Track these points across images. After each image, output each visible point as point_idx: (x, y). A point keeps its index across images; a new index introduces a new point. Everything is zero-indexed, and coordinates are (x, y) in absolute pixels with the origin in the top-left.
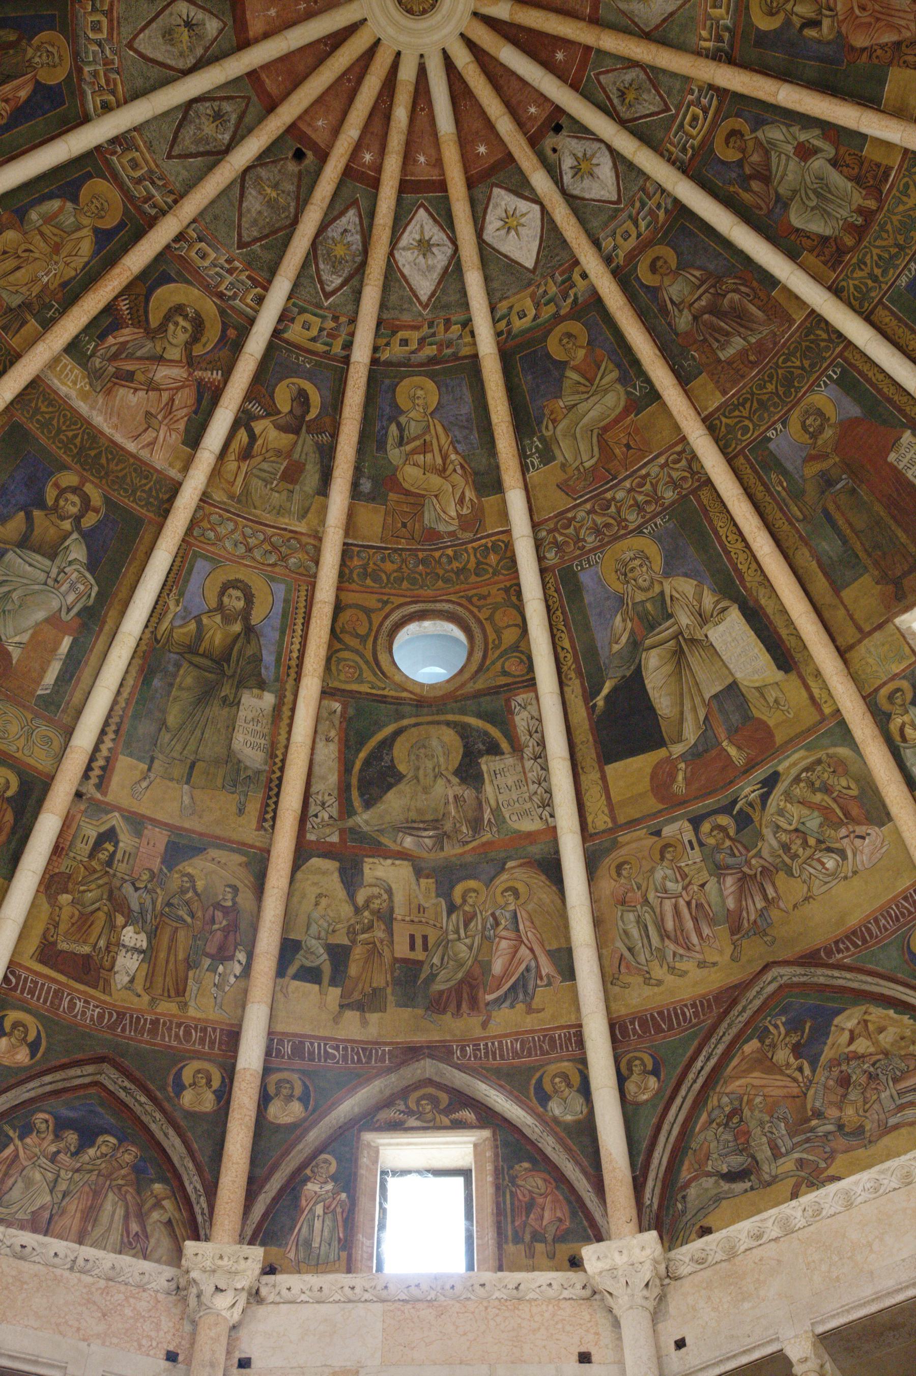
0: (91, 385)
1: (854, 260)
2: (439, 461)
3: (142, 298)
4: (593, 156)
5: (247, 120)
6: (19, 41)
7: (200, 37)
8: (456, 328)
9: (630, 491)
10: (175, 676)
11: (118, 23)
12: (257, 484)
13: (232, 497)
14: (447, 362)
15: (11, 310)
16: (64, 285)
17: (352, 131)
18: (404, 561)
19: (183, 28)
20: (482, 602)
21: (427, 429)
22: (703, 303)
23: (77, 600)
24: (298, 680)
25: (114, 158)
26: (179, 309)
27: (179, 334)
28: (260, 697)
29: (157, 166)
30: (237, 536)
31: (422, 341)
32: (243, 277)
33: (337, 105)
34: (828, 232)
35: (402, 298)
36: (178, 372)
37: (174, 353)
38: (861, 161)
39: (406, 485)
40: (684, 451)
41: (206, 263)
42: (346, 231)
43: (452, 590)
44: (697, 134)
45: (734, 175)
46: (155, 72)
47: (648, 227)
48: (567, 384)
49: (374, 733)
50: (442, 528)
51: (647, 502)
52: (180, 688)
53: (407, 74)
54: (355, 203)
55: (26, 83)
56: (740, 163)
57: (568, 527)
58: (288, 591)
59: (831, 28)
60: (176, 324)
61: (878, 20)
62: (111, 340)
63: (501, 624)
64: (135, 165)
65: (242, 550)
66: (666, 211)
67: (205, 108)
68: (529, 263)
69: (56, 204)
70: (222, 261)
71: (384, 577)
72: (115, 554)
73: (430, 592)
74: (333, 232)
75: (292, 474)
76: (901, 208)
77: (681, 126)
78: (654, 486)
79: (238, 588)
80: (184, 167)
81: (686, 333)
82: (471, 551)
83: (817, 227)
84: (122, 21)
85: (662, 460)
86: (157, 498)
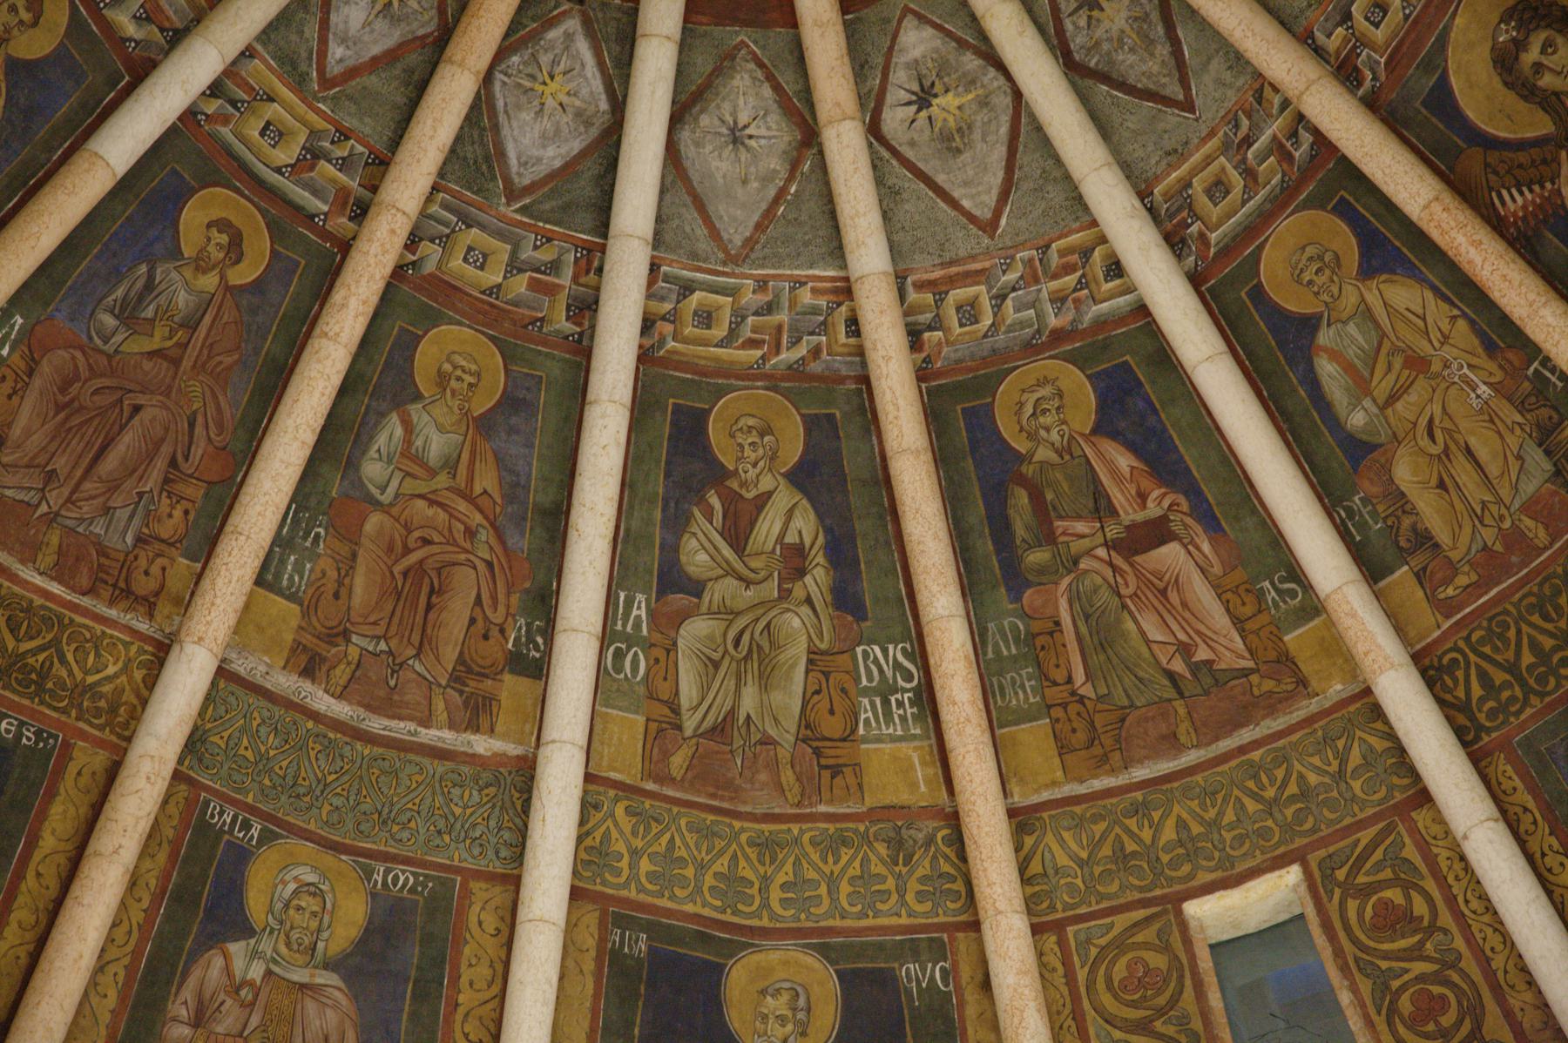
3: (1493, 157)
6: (1023, 481)
7: (943, 68)
11: (951, 263)
15: (1558, 473)
16: (1490, 348)
19: (934, 110)
25: (1213, 237)
26: (1505, 61)
29: (1212, 134)
46: (1029, 160)
55: (1101, 455)
60: (1538, 67)
64: (1219, 188)
69: (1327, 369)
80: (1205, 66)
84: (947, 256)
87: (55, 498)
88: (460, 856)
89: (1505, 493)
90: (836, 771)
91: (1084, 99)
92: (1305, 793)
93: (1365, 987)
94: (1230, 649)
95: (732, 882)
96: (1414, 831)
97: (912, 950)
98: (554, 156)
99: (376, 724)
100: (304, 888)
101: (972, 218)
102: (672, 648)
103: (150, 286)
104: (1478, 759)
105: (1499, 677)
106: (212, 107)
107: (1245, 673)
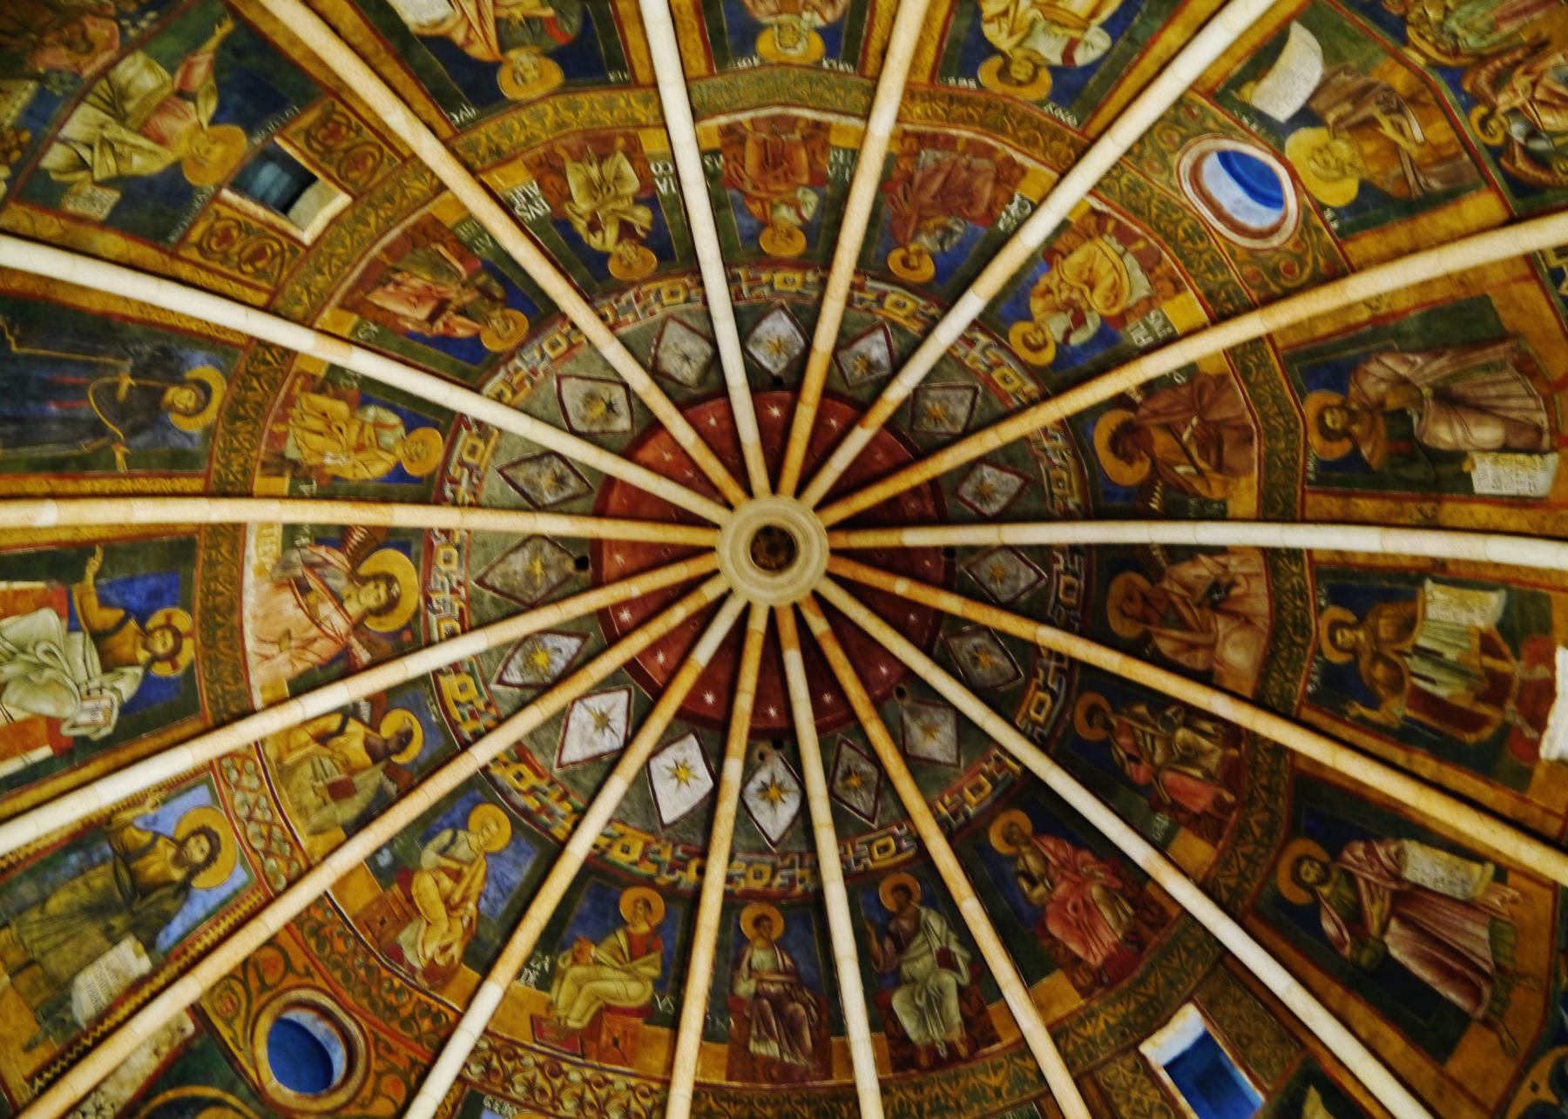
0: (274, 567)
1: (916, 1080)
2: (457, 897)
4: (786, 792)
5: (578, 505)
7: (607, 421)
8: (564, 808)
9: (586, 1081)
10: (93, 866)
12: (307, 769)
13: (279, 761)
14: (536, 825)
15: (282, 456)
16: (335, 478)
17: (635, 588)
18: (355, 953)
20: (383, 1053)
21: (471, 863)
22: (772, 989)
23: (86, 725)
24: (185, 971)
25: (465, 432)
26: (390, 579)
27: (372, 596)
28: (138, 955)
30: (251, 797)
31: (533, 790)
32: (456, 605)
33: (643, 559)
34: (914, 1036)
35: (549, 740)
36: (339, 623)
37: (353, 608)
38: (982, 1011)
39: (414, 891)
40: (657, 1092)
41: (443, 567)
42: (560, 651)
43: (370, 1017)
44: (880, 861)
45: (878, 919)
46: (555, 409)
47: (781, 886)
48: (611, 940)
49: (198, 1083)
50: (409, 955)
51: (591, 1105)
52: (86, 884)
53: (710, 592)
54: (584, 637)
56: (891, 916)
57: (509, 1058)
58: (245, 886)
59: (1041, 897)
60: (377, 587)
61: (1079, 927)
62: (322, 551)
63: (384, 1090)
64: (473, 451)
65: (243, 812)
66: (805, 891)
67: (558, 466)
68: (668, 815)
69: (392, 419)
70: (454, 578)
71: (328, 950)
72: (152, 718)
73: (348, 998)
74: (551, 641)
75: (340, 791)
76: (983, 1078)
77: (870, 843)
78: (609, 1097)
79: (210, 840)
80: (502, 490)
81: (740, 1001)
82: (414, 999)
83: (909, 1024)
85: (633, 1082)
86: (226, 703)
87: (964, 161)
88: (718, 81)
89: (298, 432)
90: (540, 164)
91: (541, 447)
92: (321, 272)
93: (255, 225)
94: (383, 299)
95: (575, 108)
96: (266, 291)
97: (471, 121)
98: (767, 325)
99: (777, 110)
100: (794, 47)
101: (570, 376)
102: (641, 178)
103: (942, 243)
104: (251, 338)
105: (263, 368)
106: (933, 311)
107: (368, 293)
